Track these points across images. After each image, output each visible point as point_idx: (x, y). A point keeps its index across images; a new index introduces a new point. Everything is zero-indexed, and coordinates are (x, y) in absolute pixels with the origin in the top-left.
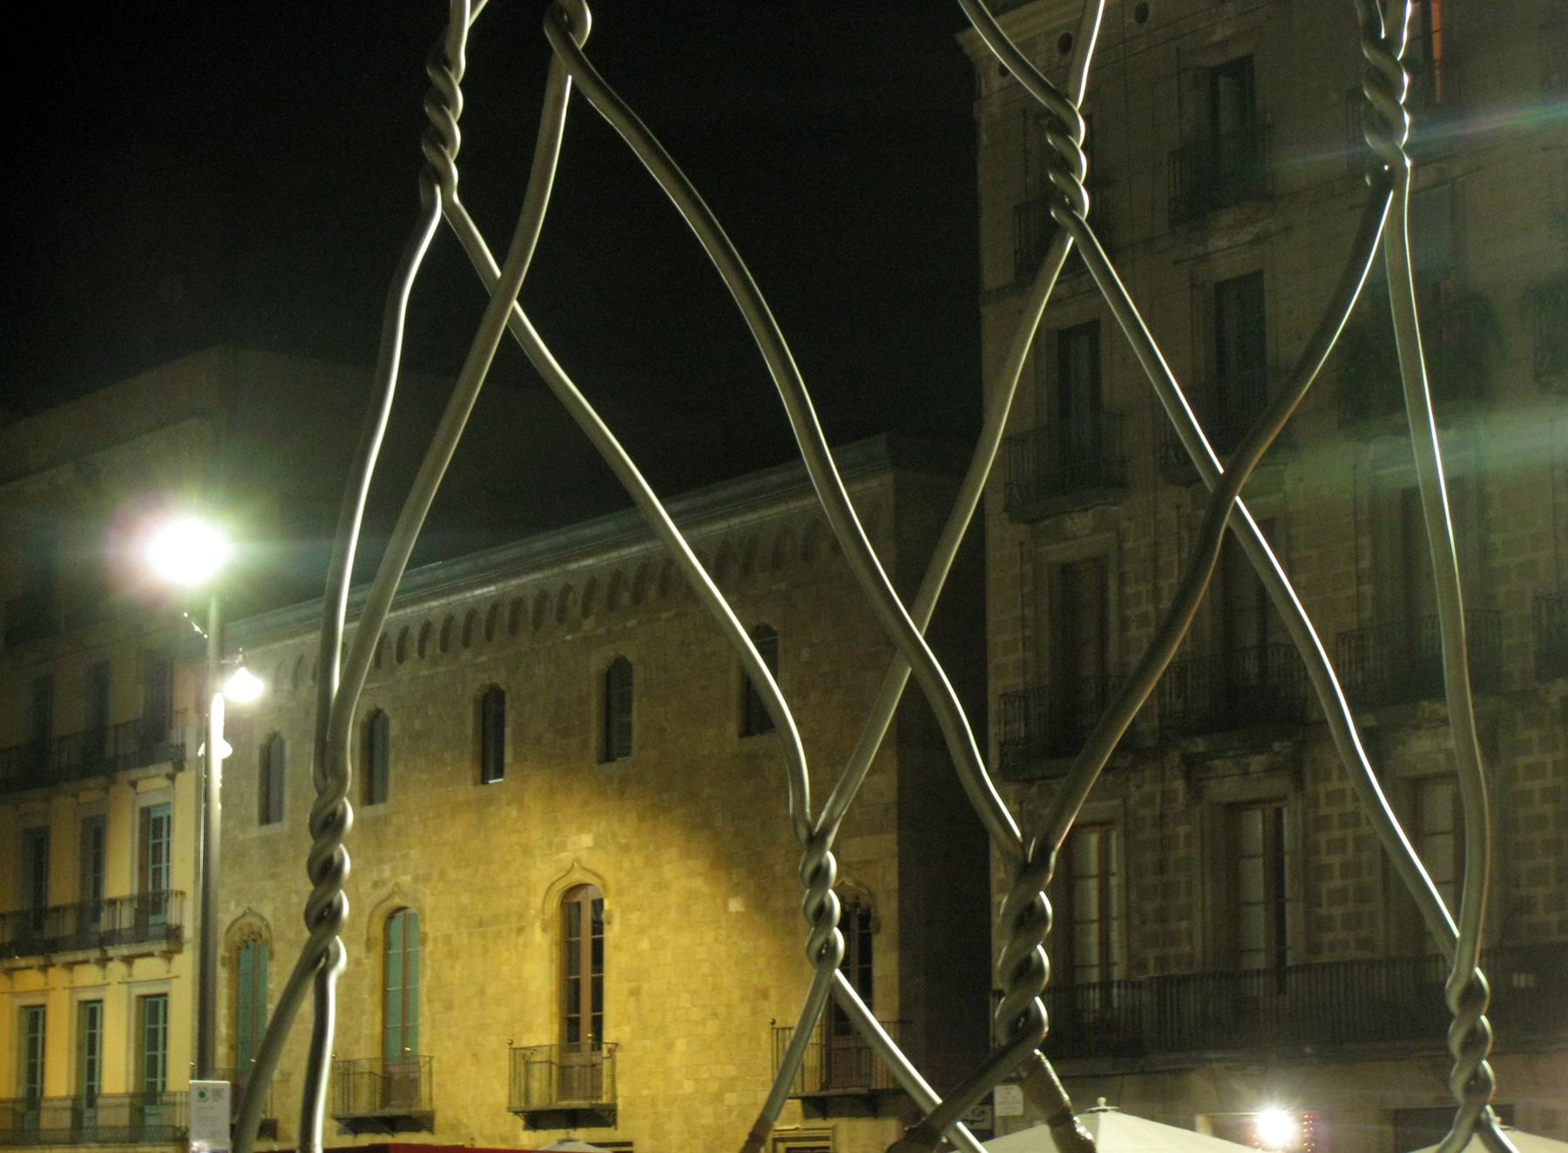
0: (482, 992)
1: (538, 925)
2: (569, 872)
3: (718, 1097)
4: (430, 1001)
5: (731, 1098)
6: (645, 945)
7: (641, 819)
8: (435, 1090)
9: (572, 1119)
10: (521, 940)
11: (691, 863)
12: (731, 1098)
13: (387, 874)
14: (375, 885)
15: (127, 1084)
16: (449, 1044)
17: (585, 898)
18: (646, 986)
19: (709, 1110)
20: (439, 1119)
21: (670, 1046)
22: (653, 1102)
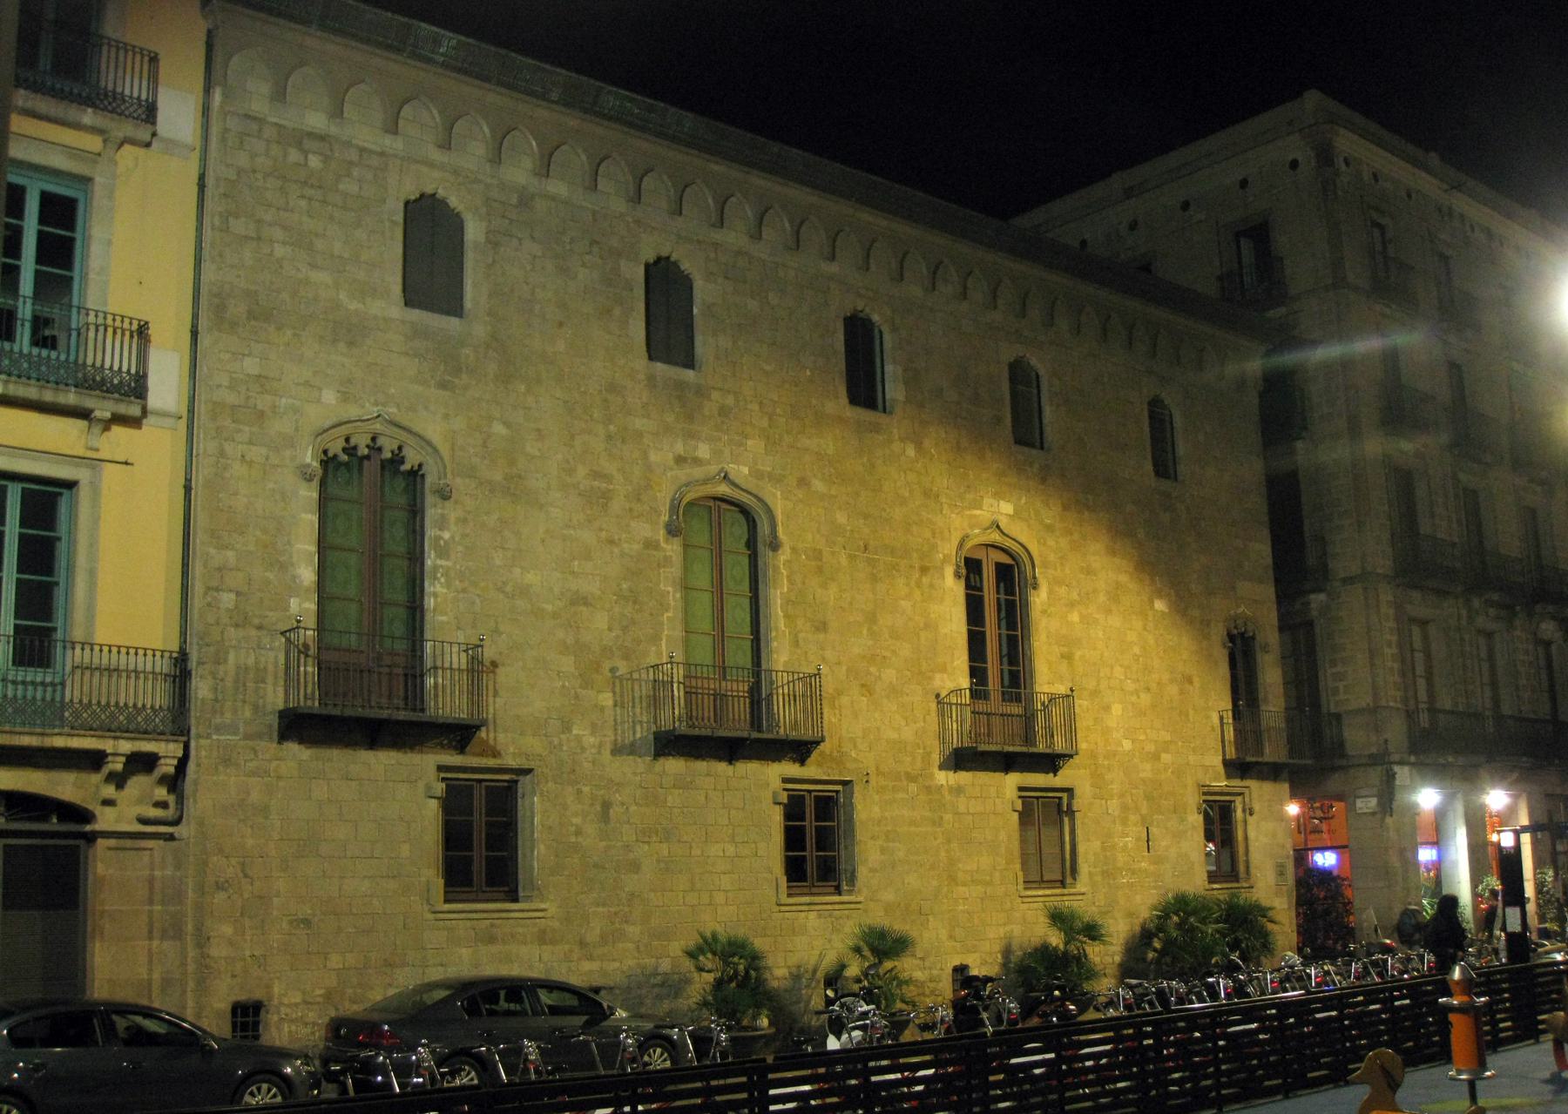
0: (872, 619)
1: (949, 571)
3: (1156, 757)
4: (787, 616)
7: (1066, 508)
9: (1007, 762)
11: (1117, 560)
12: (1166, 758)
13: (703, 451)
14: (680, 460)
17: (989, 561)
18: (1078, 654)
19: (1148, 766)
21: (1107, 708)
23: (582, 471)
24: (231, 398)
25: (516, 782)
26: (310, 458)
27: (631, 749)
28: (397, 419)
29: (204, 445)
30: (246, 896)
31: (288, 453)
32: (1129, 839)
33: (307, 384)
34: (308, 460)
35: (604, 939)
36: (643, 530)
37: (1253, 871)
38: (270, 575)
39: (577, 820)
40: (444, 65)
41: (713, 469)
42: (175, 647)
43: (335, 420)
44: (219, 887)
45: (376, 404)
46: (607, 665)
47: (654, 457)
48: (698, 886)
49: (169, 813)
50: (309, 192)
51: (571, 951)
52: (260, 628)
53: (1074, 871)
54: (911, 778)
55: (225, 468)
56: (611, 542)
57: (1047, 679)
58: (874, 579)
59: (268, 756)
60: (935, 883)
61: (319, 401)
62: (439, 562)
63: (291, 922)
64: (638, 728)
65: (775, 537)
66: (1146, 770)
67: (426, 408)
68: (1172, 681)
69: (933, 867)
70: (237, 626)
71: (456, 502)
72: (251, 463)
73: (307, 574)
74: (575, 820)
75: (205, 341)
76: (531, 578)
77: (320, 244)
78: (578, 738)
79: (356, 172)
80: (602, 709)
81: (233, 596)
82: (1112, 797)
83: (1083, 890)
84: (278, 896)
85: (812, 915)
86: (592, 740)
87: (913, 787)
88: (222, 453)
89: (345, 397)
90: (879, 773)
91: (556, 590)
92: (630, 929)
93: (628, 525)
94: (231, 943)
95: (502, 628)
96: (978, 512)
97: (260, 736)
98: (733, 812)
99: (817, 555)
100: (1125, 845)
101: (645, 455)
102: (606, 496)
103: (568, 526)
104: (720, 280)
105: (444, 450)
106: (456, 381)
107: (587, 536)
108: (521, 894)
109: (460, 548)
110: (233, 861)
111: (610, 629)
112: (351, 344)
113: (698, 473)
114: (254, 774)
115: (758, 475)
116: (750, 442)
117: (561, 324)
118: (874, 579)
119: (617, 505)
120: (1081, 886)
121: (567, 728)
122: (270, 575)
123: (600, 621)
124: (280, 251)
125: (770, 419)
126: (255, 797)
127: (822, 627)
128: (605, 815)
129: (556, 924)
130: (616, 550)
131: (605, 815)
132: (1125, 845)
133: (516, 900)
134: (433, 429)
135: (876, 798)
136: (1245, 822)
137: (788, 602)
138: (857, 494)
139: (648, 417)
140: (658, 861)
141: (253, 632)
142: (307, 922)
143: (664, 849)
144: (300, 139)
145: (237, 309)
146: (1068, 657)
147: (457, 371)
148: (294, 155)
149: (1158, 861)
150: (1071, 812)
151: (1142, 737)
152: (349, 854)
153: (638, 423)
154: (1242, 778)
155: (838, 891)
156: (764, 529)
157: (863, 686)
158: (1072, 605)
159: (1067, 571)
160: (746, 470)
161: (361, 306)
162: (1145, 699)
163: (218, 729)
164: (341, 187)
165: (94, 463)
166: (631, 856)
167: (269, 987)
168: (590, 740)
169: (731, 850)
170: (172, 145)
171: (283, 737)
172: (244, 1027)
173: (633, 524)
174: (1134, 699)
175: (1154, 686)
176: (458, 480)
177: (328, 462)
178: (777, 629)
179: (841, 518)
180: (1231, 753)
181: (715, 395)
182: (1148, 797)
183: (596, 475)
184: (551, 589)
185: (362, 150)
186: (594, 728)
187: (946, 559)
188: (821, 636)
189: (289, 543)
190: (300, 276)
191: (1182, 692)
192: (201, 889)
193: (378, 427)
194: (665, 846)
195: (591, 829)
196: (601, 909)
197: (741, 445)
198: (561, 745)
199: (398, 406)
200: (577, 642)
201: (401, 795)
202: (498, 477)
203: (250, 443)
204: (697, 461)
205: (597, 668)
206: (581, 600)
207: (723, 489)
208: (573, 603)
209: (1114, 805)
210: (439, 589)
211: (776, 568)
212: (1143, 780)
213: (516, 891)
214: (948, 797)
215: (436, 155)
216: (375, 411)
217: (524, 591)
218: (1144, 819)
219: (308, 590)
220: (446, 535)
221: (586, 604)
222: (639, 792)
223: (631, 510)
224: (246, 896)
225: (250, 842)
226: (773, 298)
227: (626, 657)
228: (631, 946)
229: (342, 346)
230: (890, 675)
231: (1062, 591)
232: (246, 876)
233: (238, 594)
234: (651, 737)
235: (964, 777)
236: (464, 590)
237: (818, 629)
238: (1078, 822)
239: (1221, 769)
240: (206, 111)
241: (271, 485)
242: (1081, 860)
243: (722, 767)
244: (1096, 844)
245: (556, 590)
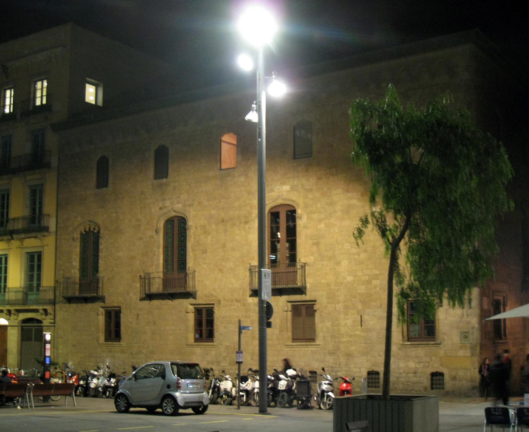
0: (224, 246)
2: (277, 199)
3: (369, 282)
4: (193, 250)
5: (374, 282)
6: (322, 226)
7: (319, 179)
8: (197, 283)
10: (247, 226)
11: (350, 195)
12: (374, 282)
15: (21, 283)
16: (205, 266)
19: (363, 287)
20: (199, 294)
21: (338, 263)
22: (328, 285)
44: (60, 337)
54: (238, 301)
66: (362, 289)
73: (76, 263)
74: (130, 320)
82: (339, 303)
85: (198, 349)
87: (239, 304)
100: (346, 324)
131: (138, 318)
132: (346, 324)
146: (317, 244)
157: (219, 270)
158: (320, 221)
165: (43, 247)
169: (173, 327)
174: (356, 257)
206: (133, 258)
209: (340, 307)
218: (359, 312)
230: (230, 264)
231: (315, 216)
237: (203, 253)
243: (169, 302)
244: (328, 324)
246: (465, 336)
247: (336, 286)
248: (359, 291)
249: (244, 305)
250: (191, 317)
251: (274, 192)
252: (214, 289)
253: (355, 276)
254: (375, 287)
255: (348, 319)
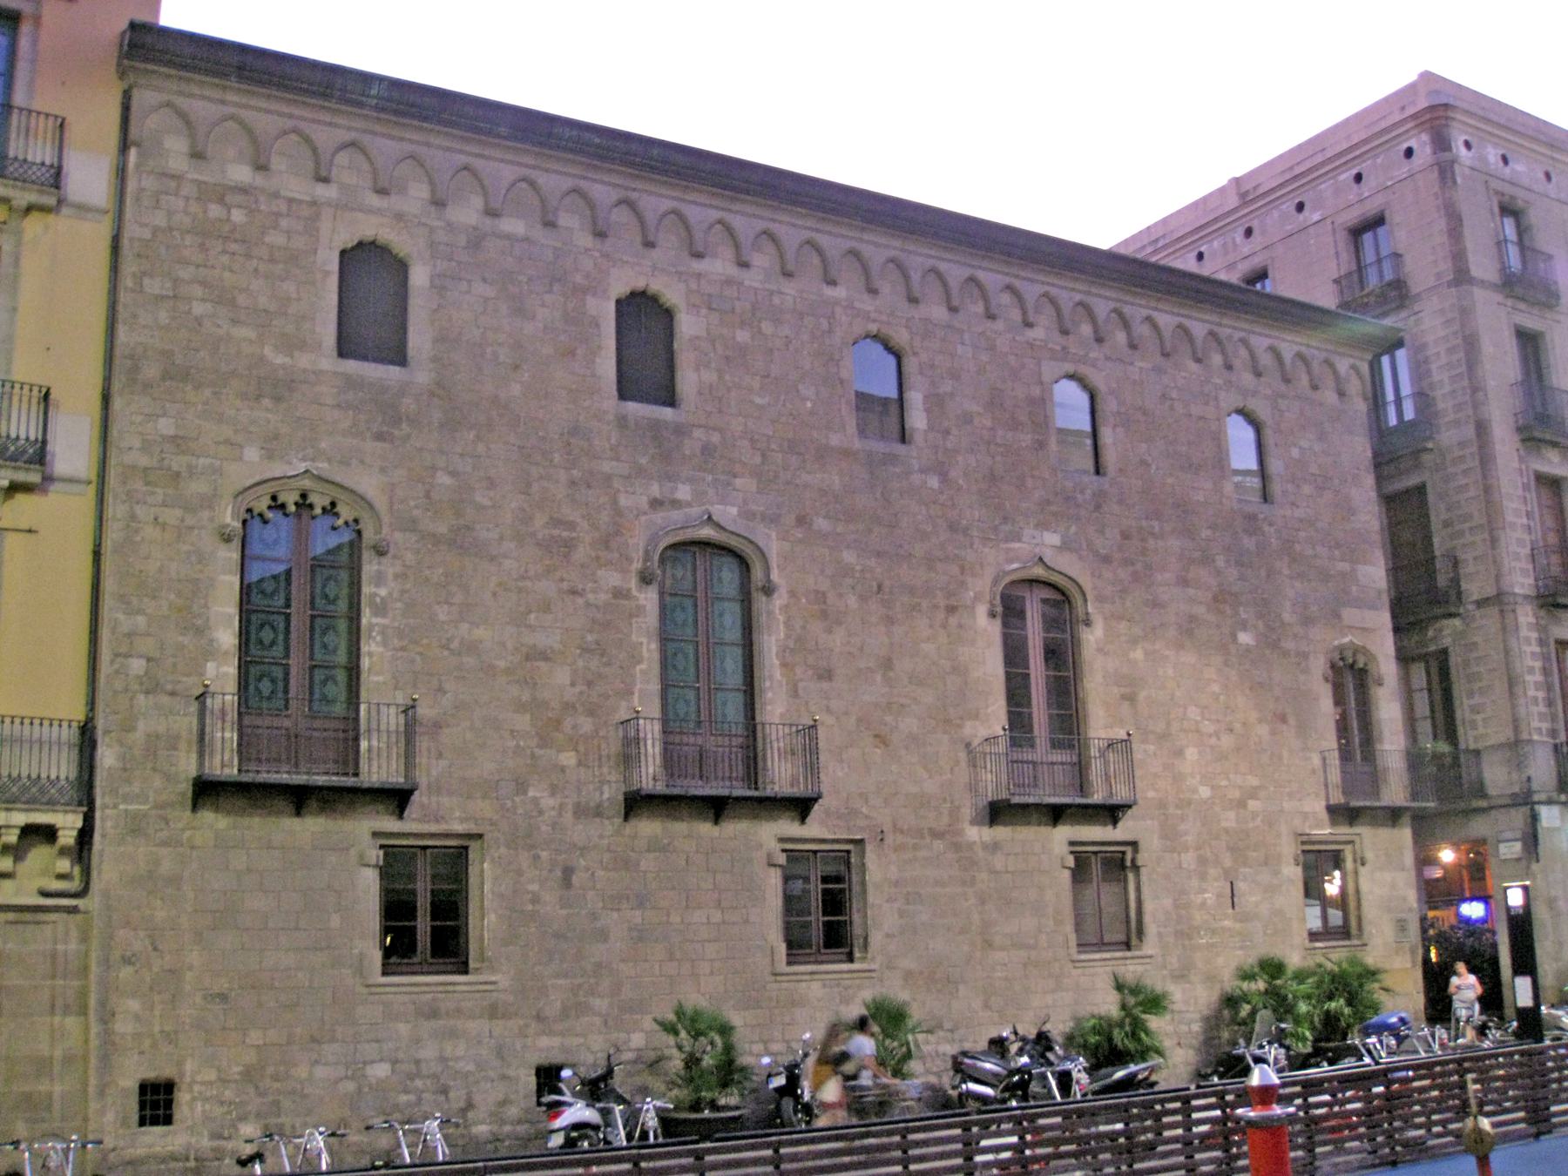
0: (887, 664)
1: (982, 610)
4: (784, 665)
6: (1138, 654)
9: (1056, 814)
10: (953, 621)
13: (684, 492)
14: (656, 504)
18: (1142, 695)
19: (1232, 815)
21: (1179, 753)
23: (540, 520)
24: (144, 461)
25: (466, 848)
26: (230, 519)
27: (598, 812)
28: (325, 475)
29: (116, 510)
30: (155, 970)
31: (206, 514)
32: (1211, 894)
33: (228, 442)
34: (228, 520)
35: (565, 1013)
36: (613, 579)
37: (1367, 928)
38: (185, 640)
39: (534, 887)
40: (377, 108)
41: (695, 511)
42: (82, 717)
43: (257, 478)
44: (127, 961)
45: (304, 459)
46: (568, 723)
47: (623, 501)
48: (678, 955)
49: (74, 885)
50: (234, 247)
51: (527, 1026)
52: (173, 694)
53: (1140, 932)
54: (936, 835)
55: (137, 531)
56: (574, 592)
57: (1100, 726)
58: (890, 621)
59: (180, 825)
60: (966, 948)
61: (241, 459)
62: (374, 620)
63: (205, 998)
64: (606, 788)
65: (769, 581)
66: (1229, 819)
67: (362, 462)
68: (1260, 721)
69: (963, 931)
70: (147, 692)
71: (395, 557)
72: (164, 526)
73: (227, 638)
75: (117, 403)
76: (480, 633)
77: (242, 300)
78: (535, 801)
79: (284, 223)
80: (563, 769)
81: (143, 662)
82: (1186, 849)
83: (1150, 952)
84: (190, 968)
85: (816, 986)
86: (551, 802)
87: (939, 845)
88: (133, 517)
89: (270, 455)
90: (896, 829)
91: (510, 645)
92: (597, 1003)
93: (594, 574)
94: (137, 1018)
95: (447, 686)
96: (1017, 545)
97: (172, 805)
98: (718, 876)
99: (821, 597)
100: (1203, 904)
101: (615, 502)
102: (569, 545)
103: (523, 578)
104: (704, 311)
105: (381, 503)
106: (396, 432)
107: (546, 587)
108: (472, 964)
109: (399, 605)
110: (142, 934)
111: (573, 684)
112: (278, 399)
113: (676, 516)
114: (164, 844)
115: (748, 515)
116: (738, 482)
117: (516, 367)
118: (890, 621)
119: (581, 553)
120: (1150, 947)
121: (521, 787)
122: (185, 640)
123: (562, 676)
124: (198, 309)
125: (763, 455)
126: (166, 867)
127: (827, 675)
128: (566, 881)
129: (511, 998)
130: (580, 601)
131: (566, 881)
132: (1203, 904)
133: (466, 972)
134: (368, 484)
135: (893, 857)
136: (1356, 873)
137: (784, 649)
138: (870, 531)
139: (618, 459)
140: (630, 929)
141: (165, 699)
142: (223, 997)
143: (637, 916)
144: (222, 194)
145: (151, 371)
146: (1131, 698)
147: (397, 421)
148: (215, 210)
149: (1245, 918)
150: (1136, 868)
151: (1224, 783)
152: (271, 925)
153: (607, 467)
154: (1351, 825)
155: (850, 958)
156: (757, 573)
157: (876, 736)
158: (1134, 641)
159: (1128, 604)
160: (734, 511)
161: (287, 360)
162: (1227, 741)
163: (126, 798)
164: (267, 239)
166: (599, 925)
167: (180, 1064)
168: (548, 802)
169: (717, 916)
170: (83, 209)
171: (195, 807)
172: (155, 1105)
173: (599, 573)
175: (1237, 726)
176: (398, 536)
177: (250, 517)
178: (771, 677)
179: (849, 557)
180: (1337, 798)
181: (698, 433)
182: (1232, 849)
183: (557, 522)
184: (503, 644)
185: (291, 201)
186: (553, 790)
187: (977, 598)
188: (825, 685)
189: (206, 606)
190: (221, 332)
191: (1273, 733)
192: (106, 963)
193: (307, 483)
194: (638, 913)
195: (550, 897)
196: (560, 982)
197: (729, 484)
198: (515, 808)
199: (329, 460)
200: (534, 699)
201: (345, 862)
202: (442, 529)
203: (164, 504)
204: (676, 504)
205: (557, 724)
207: (707, 532)
208: (528, 658)
209: (1189, 859)
210: (374, 648)
211: (770, 613)
212: (1227, 831)
213: (466, 963)
214: (981, 854)
215: (374, 200)
216: (302, 467)
217: (472, 647)
218: (1226, 872)
219: (226, 653)
220: (383, 592)
221: (547, 659)
222: (607, 857)
223: (598, 558)
224: (155, 970)
225: (160, 915)
226: (767, 327)
227: (591, 713)
228: (597, 1020)
229: (266, 402)
230: (909, 724)
231: (1123, 626)
232: (155, 949)
233: (149, 660)
234: (621, 798)
235: (1001, 832)
236: (403, 649)
237: (820, 677)
238: (1144, 878)
239: (1324, 815)
240: (121, 173)
241: (186, 548)
242: (1147, 919)
245: (510, 645)
246: (1401, 926)
247: (1177, 807)
248: (1224, 824)
249: (957, 847)
250: (369, 884)
251: (1020, 540)
252: (864, 797)
253: (1213, 787)
254: (1254, 815)
255: (1205, 891)
